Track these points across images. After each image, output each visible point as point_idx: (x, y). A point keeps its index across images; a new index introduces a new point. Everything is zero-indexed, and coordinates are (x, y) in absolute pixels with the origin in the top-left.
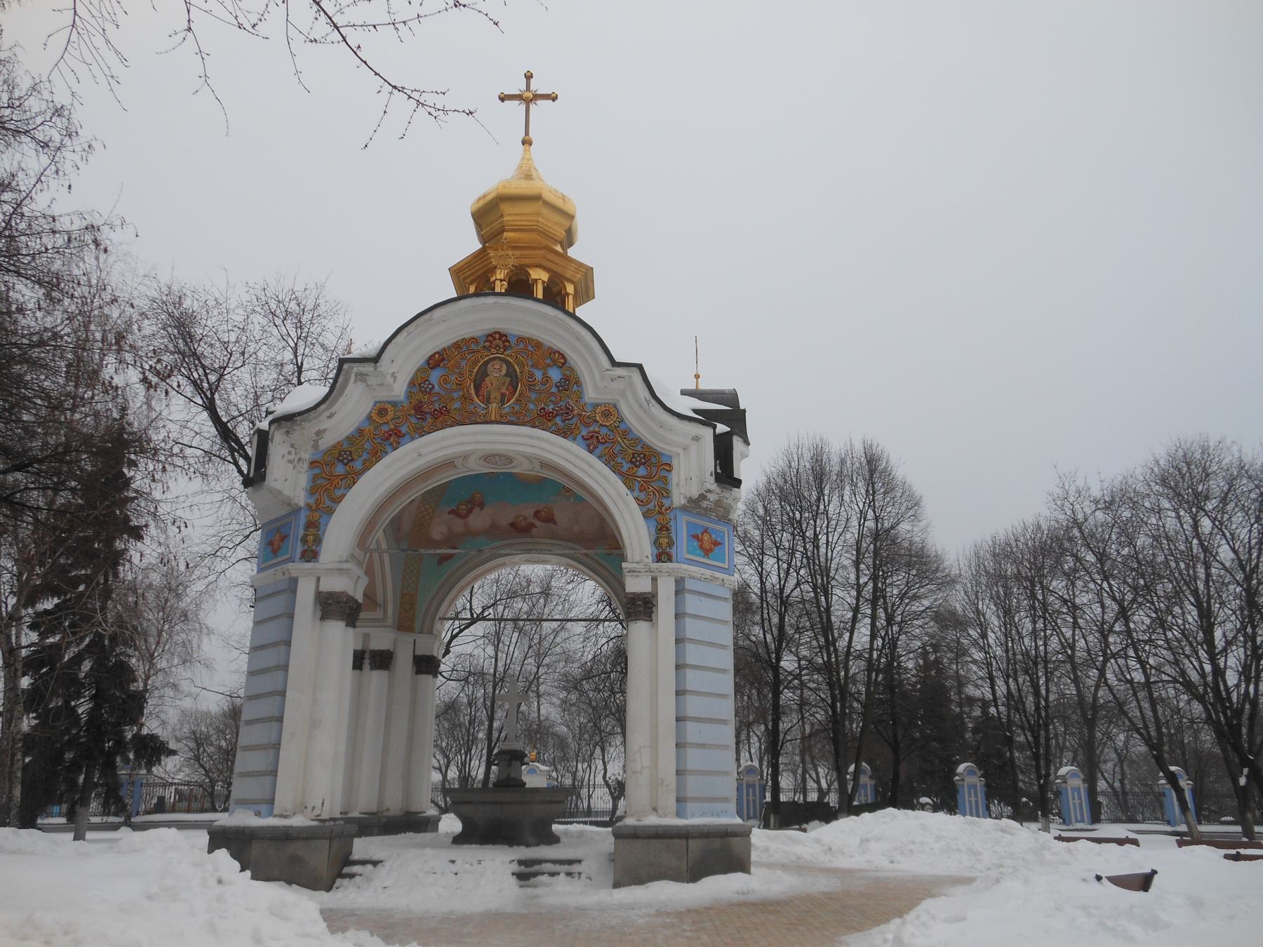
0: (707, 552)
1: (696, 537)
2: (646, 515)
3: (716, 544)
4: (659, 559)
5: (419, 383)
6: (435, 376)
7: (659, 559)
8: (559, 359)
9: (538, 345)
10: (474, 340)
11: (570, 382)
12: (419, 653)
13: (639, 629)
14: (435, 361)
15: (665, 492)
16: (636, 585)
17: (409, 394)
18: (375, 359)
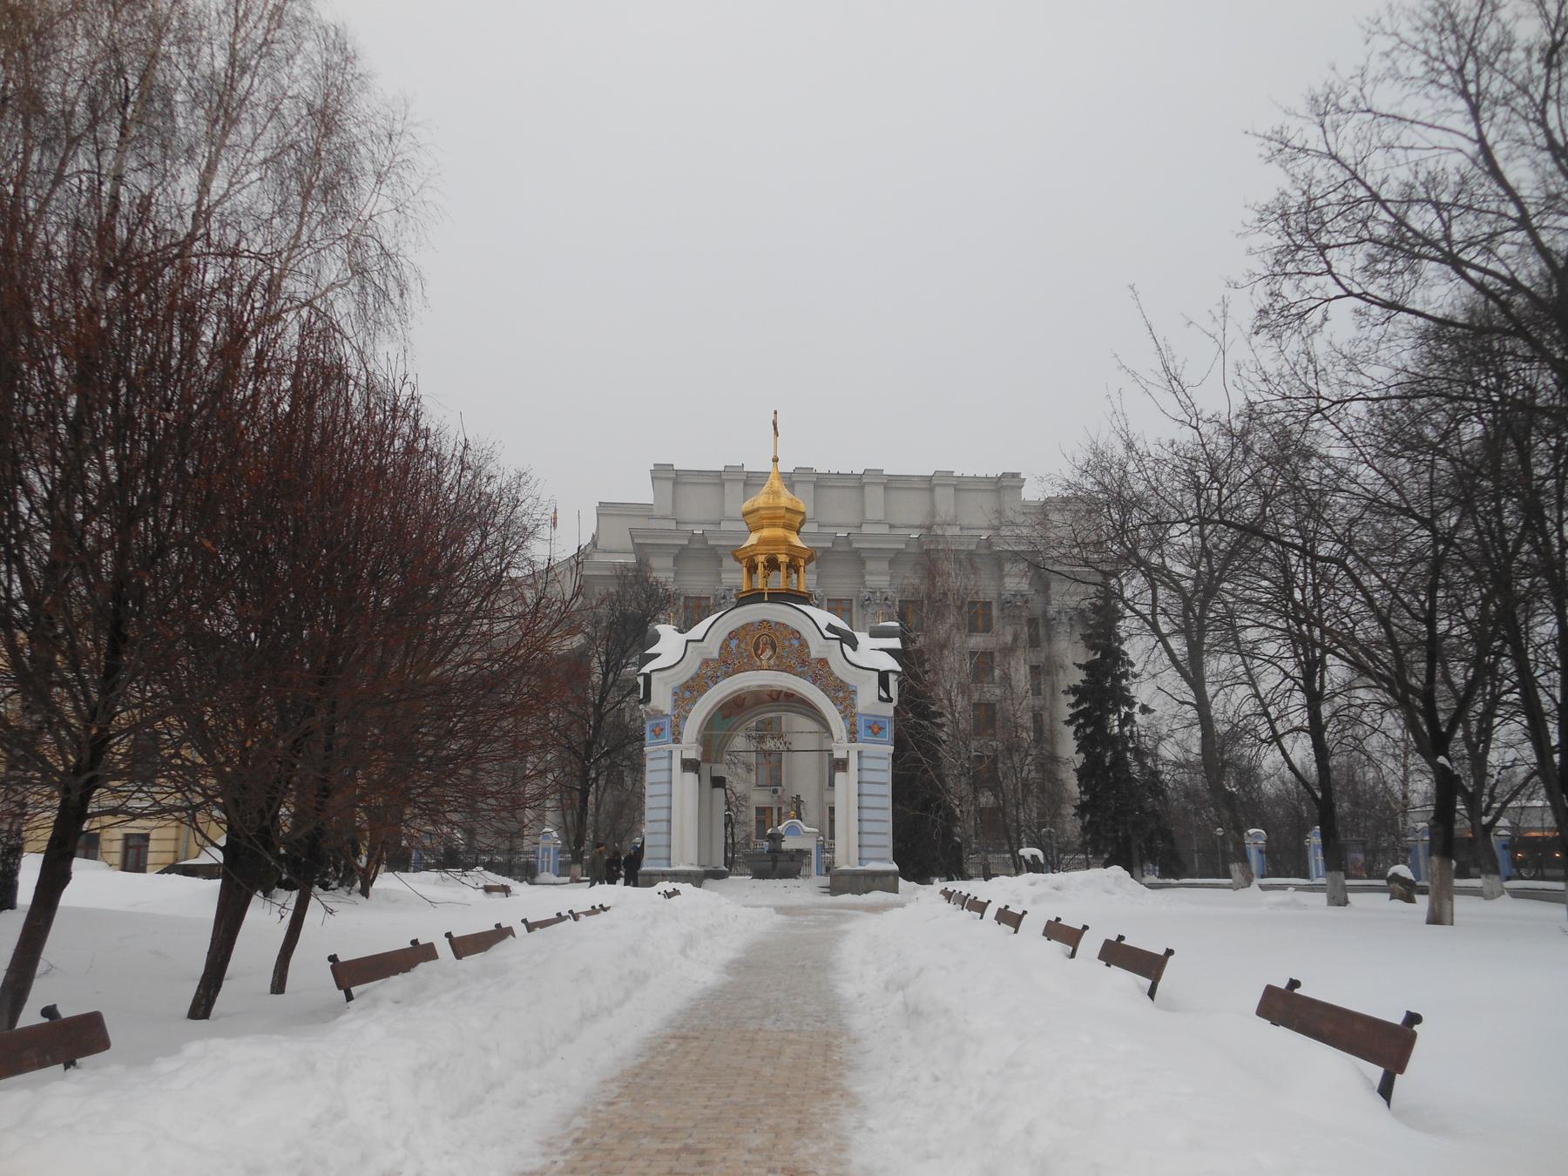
0: (875, 734)
1: (870, 727)
2: (843, 718)
3: (880, 729)
4: (850, 741)
5: (725, 646)
6: (734, 643)
7: (850, 741)
8: (796, 634)
9: (785, 626)
10: (752, 624)
11: (804, 644)
12: (715, 775)
13: (839, 776)
14: (732, 635)
15: (853, 705)
16: (839, 754)
17: (720, 654)
18: (702, 640)
